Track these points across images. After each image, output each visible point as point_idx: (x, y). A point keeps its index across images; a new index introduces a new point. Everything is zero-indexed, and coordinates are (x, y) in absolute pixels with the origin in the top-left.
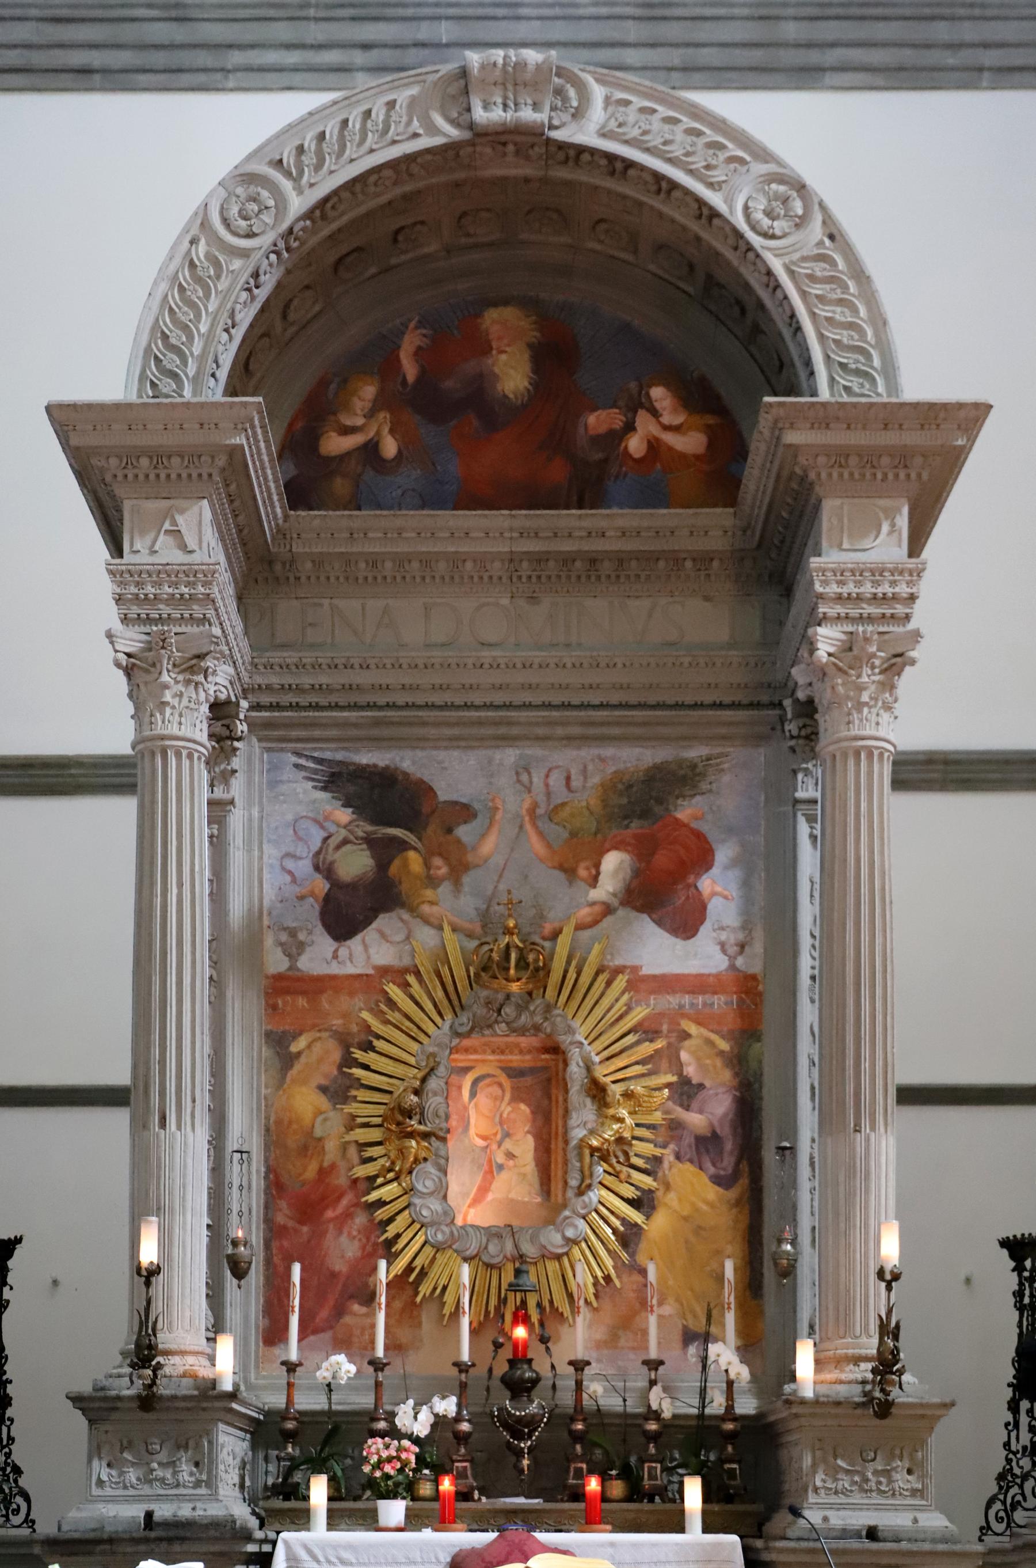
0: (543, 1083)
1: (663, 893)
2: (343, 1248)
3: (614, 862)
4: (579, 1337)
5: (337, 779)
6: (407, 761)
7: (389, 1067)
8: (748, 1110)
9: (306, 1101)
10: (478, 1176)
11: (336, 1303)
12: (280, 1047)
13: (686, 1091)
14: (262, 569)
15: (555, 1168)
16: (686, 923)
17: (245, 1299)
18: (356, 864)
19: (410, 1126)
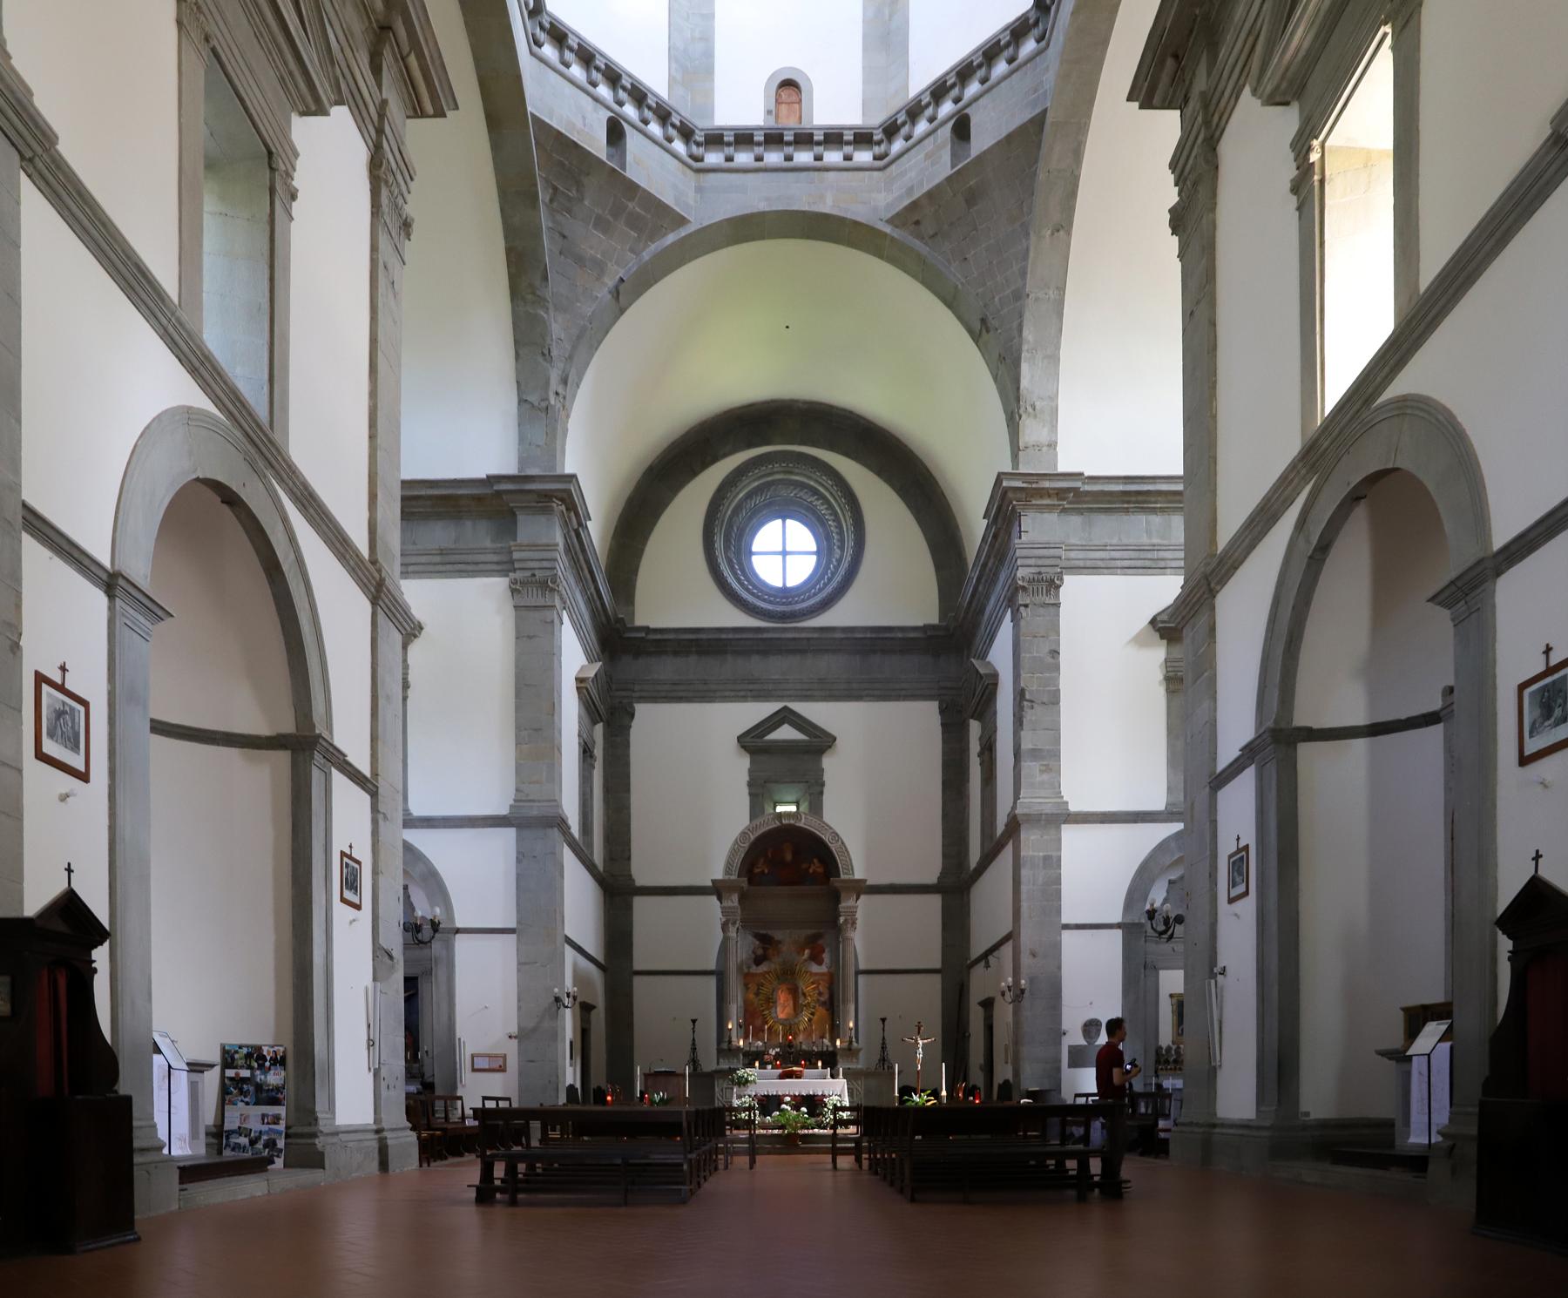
0: (794, 992)
1: (816, 958)
2: (758, 1022)
3: (807, 952)
4: (801, 1038)
5: (757, 936)
6: (770, 932)
7: (764, 990)
8: (832, 997)
9: (752, 996)
10: (782, 1010)
11: (758, 1033)
12: (746, 986)
13: (820, 994)
14: (743, 898)
15: (797, 1008)
16: (820, 963)
17: (742, 1031)
18: (760, 952)
19: (770, 1001)
